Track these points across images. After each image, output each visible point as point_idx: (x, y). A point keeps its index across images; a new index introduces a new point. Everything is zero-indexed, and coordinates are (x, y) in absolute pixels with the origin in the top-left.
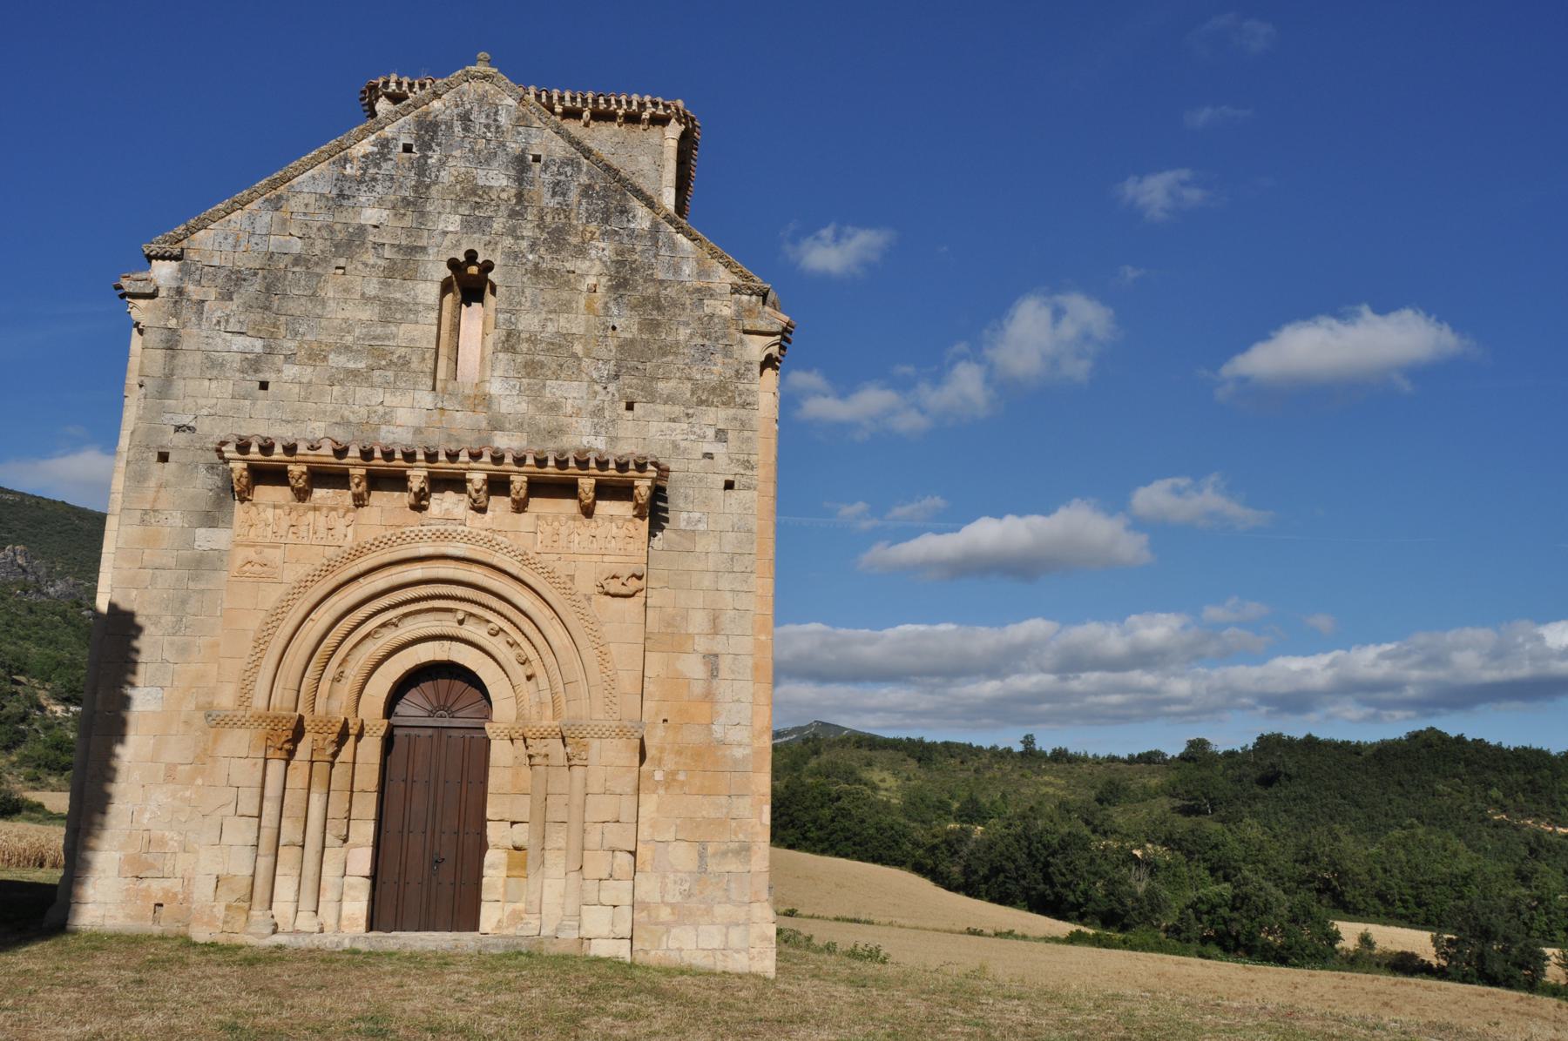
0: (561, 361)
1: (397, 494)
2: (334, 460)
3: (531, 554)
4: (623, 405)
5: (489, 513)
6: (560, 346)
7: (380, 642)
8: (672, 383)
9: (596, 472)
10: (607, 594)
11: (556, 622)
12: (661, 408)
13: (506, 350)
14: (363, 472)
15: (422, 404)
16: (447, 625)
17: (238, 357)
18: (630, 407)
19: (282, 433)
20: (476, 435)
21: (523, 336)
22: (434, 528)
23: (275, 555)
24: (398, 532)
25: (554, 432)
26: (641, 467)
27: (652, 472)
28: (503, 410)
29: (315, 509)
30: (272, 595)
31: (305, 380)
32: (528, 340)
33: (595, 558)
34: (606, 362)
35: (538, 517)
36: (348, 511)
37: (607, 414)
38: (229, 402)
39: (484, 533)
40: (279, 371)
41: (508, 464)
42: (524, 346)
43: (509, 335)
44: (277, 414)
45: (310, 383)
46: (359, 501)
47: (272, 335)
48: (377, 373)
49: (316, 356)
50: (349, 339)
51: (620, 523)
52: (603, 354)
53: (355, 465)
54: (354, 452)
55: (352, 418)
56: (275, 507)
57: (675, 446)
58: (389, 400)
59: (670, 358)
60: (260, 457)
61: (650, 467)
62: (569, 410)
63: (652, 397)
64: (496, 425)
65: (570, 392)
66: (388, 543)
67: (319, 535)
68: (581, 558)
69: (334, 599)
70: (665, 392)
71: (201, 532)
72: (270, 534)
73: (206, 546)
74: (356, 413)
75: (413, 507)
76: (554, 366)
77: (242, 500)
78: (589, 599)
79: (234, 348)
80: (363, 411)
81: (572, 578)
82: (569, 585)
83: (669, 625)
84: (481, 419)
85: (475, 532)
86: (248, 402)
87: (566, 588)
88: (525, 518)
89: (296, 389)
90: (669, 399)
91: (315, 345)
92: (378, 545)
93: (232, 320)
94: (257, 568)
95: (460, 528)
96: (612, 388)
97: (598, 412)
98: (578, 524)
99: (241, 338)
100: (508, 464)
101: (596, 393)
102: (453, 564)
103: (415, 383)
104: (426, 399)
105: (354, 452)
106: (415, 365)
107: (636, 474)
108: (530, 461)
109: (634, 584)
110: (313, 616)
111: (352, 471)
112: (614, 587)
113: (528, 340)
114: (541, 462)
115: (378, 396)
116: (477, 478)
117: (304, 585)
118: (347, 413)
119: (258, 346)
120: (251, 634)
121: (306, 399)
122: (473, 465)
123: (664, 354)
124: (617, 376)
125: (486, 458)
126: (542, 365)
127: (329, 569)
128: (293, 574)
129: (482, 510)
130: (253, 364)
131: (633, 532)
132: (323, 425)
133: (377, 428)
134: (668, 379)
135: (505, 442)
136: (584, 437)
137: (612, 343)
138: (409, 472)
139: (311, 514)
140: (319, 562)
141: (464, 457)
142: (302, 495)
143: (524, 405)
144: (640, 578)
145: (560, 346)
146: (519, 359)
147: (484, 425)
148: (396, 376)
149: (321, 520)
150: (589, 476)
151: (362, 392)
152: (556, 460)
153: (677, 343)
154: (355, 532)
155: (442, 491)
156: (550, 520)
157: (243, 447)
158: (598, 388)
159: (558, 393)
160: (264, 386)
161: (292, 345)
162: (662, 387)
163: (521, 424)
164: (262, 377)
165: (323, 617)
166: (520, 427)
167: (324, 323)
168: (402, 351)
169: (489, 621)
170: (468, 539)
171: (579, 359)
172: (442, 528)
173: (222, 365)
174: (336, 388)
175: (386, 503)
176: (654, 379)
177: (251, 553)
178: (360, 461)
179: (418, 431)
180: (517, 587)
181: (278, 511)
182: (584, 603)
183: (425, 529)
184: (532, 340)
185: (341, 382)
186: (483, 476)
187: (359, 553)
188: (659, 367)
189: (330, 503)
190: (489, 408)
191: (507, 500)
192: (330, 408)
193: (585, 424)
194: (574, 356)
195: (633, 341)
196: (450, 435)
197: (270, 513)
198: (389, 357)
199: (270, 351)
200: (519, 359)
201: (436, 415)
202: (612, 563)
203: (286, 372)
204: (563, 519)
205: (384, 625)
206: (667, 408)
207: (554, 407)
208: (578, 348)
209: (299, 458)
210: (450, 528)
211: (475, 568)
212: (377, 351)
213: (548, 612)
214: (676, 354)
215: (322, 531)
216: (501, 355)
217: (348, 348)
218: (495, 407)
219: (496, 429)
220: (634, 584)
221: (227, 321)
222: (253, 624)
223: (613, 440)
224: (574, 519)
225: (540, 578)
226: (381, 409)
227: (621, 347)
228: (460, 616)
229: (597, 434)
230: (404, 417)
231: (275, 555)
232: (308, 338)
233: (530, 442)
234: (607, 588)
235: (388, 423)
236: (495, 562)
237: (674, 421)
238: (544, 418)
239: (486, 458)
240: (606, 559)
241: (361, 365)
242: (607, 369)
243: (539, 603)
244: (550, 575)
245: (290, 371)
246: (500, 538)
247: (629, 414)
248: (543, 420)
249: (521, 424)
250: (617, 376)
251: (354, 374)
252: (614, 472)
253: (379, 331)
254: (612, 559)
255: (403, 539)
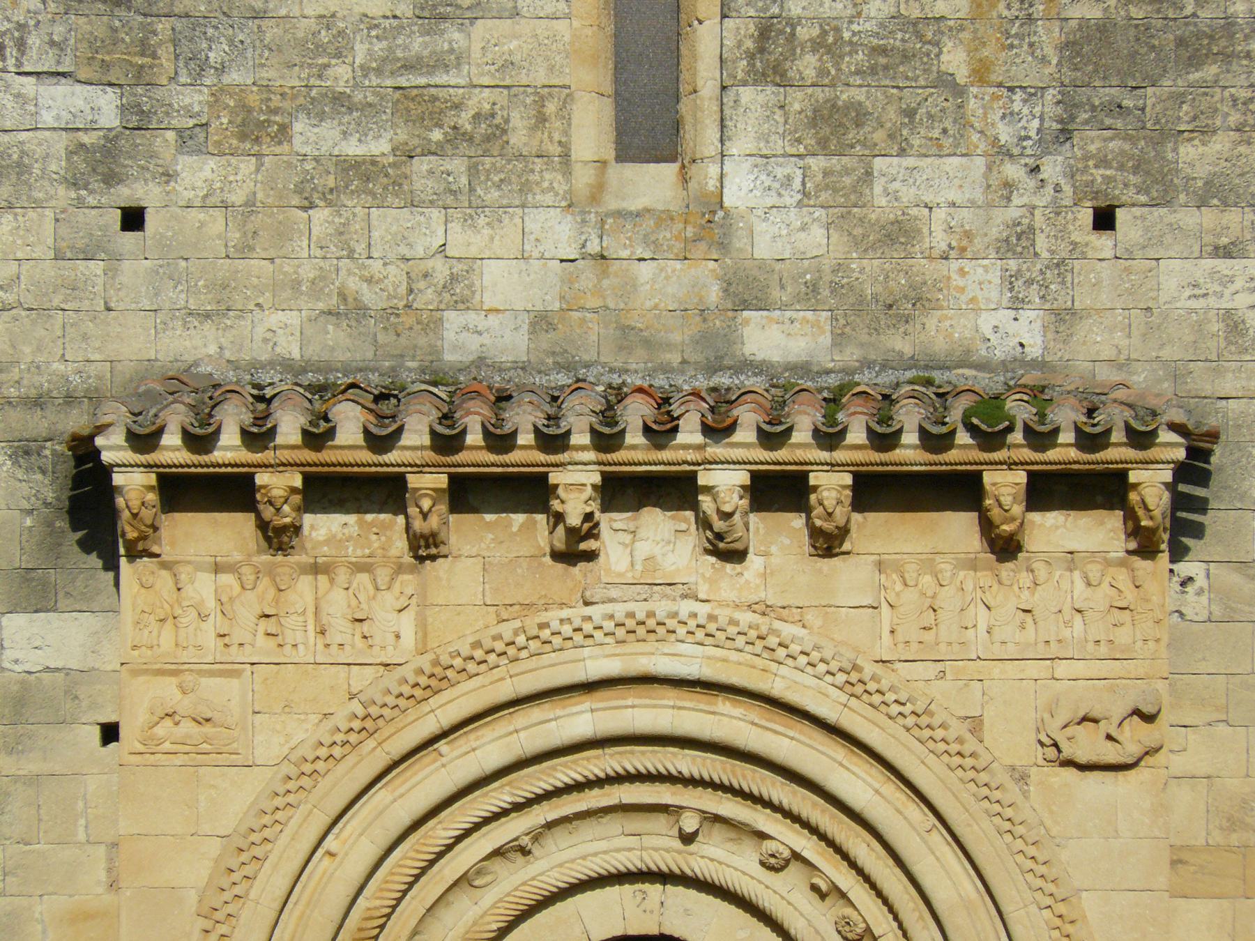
0: (910, 98)
1: (519, 518)
2: (366, 456)
3: (869, 669)
4: (1086, 216)
5: (754, 562)
6: (906, 57)
7: (489, 898)
8: (1220, 144)
9: (1027, 454)
10: (1069, 763)
11: (938, 838)
12: (1189, 218)
13: (758, 78)
14: (442, 481)
15: (549, 248)
16: (657, 846)
17: (61, 143)
18: (1104, 220)
19: (202, 347)
20: (695, 326)
21: (803, 33)
22: (619, 610)
23: (223, 694)
24: (531, 624)
25: (911, 303)
26: (1141, 439)
27: (1172, 448)
28: (763, 250)
29: (316, 569)
30: (234, 799)
31: (237, 198)
32: (818, 45)
33: (1033, 669)
34: (1034, 94)
35: (880, 566)
36: (400, 569)
37: (1042, 244)
38: (49, 270)
39: (746, 618)
40: (169, 176)
41: (801, 446)
42: (808, 65)
43: (765, 33)
44: (174, 296)
45: (250, 203)
46: (425, 548)
47: (141, 77)
48: (422, 165)
49: (257, 128)
50: (340, 75)
51: (1094, 571)
52: (1026, 71)
53: (420, 468)
54: (416, 435)
55: (369, 296)
56: (217, 569)
57: (1234, 325)
58: (462, 241)
59: (1211, 70)
60: (184, 456)
61: (1165, 436)
62: (940, 241)
63: (1162, 189)
64: (746, 293)
65: (937, 187)
66: (508, 652)
67: (335, 637)
68: (996, 669)
69: (380, 796)
70: (1202, 171)
71: (18, 625)
72: (210, 641)
73: (34, 660)
74: (379, 281)
75: (557, 556)
76: (892, 114)
77: (133, 556)
78: (1023, 778)
79: (47, 118)
80: (395, 274)
81: (976, 725)
82: (971, 745)
83: (1233, 824)
84: (702, 279)
85: (723, 614)
86: (97, 267)
87: (966, 762)
88: (849, 576)
89: (216, 223)
90: (1213, 193)
91: (253, 99)
92: (482, 657)
93: (34, 41)
94: (187, 727)
95: (686, 607)
96: (1052, 169)
97: (1018, 240)
98: (985, 578)
99: (61, 90)
100: (801, 446)
101: (1009, 186)
102: (670, 696)
103: (525, 188)
104: (557, 232)
105: (416, 435)
106: (519, 137)
107: (1131, 453)
108: (857, 435)
109: (1134, 737)
110: (330, 843)
111: (413, 481)
112: (1087, 745)
113: (818, 45)
114: (884, 440)
115: (430, 231)
116: (726, 484)
117: (305, 772)
118: (353, 284)
119: (106, 107)
120: (192, 897)
121: (245, 250)
122: (716, 451)
123: (1195, 61)
124: (1065, 134)
125: (745, 434)
126: (859, 115)
127: (368, 725)
128: (278, 739)
129: (736, 556)
130: (101, 161)
131: (1130, 596)
132: (293, 318)
133: (433, 325)
134: (1206, 132)
135: (772, 339)
136: (987, 321)
137: (1048, 37)
138: (554, 478)
139: (305, 583)
140: (343, 713)
141: (690, 434)
142: (278, 538)
143: (818, 233)
144: (1149, 718)
145: (906, 57)
146: (797, 101)
147: (714, 294)
148: (473, 170)
149: (337, 603)
150: (1011, 465)
151: (387, 222)
152: (923, 433)
153: (1229, 25)
154: (422, 627)
155: (637, 507)
156: (911, 571)
157: (144, 441)
158: (1013, 171)
159: (908, 194)
160: (133, 219)
161: (194, 99)
162: (1197, 158)
163: (814, 288)
164: (128, 194)
165: (357, 843)
166: (810, 295)
167: (272, 32)
168: (481, 100)
169: (762, 836)
170: (706, 633)
171: (959, 91)
172: (640, 610)
173: (22, 168)
174: (320, 215)
175: (498, 547)
176: (1167, 134)
177: (167, 691)
178: (430, 456)
179: (541, 322)
180: (838, 751)
181: (227, 579)
182: (1013, 792)
183: (595, 611)
184: (829, 43)
185: (330, 197)
186: (742, 477)
187: (437, 680)
188: (1179, 98)
189: (354, 553)
190: (724, 246)
191: (797, 521)
192: (308, 272)
193: (981, 278)
194: (946, 82)
195: (1104, 29)
196: (625, 330)
197: (203, 587)
198: (450, 120)
199: (139, 120)
200: (797, 101)
201: (587, 274)
202: (1078, 682)
203: (186, 177)
204: (946, 568)
205: (498, 853)
206: (1208, 217)
207: (899, 234)
208: (955, 60)
209: (285, 455)
210: (662, 608)
211: (724, 705)
212: (422, 108)
213: (916, 812)
214: (1227, 57)
215: (340, 629)
216: (747, 94)
217: (340, 101)
218: (740, 242)
219: (746, 305)
220: (1134, 737)
221: (21, 45)
222: (193, 871)
223: (1063, 319)
224: (973, 565)
225: (895, 728)
226: (441, 269)
227: (1070, 48)
228: (690, 823)
229: (1017, 304)
230: (506, 279)
231: (223, 694)
232: (234, 77)
233: (839, 339)
234: (1067, 751)
235: (462, 304)
236: (777, 688)
237: (1225, 252)
238: (873, 265)
239: (745, 434)
240: (1062, 669)
241: (379, 146)
242: (1035, 117)
243: (892, 790)
244: (920, 721)
245: (197, 173)
246: (788, 630)
247: (1103, 243)
248: (869, 271)
249: (814, 288)
250: (1065, 134)
251: (360, 174)
252: (1073, 453)
253: (417, 45)
254: (1079, 668)
255: (544, 641)
